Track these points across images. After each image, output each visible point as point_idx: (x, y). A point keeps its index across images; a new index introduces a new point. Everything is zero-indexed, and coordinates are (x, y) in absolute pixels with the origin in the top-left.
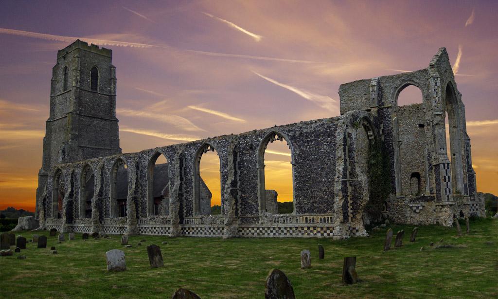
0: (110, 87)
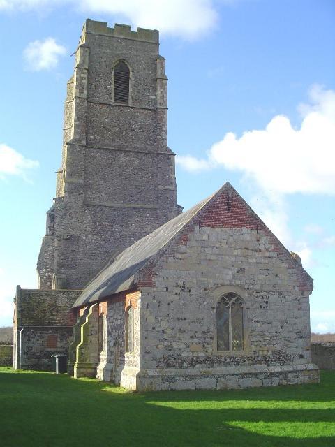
0: (156, 96)
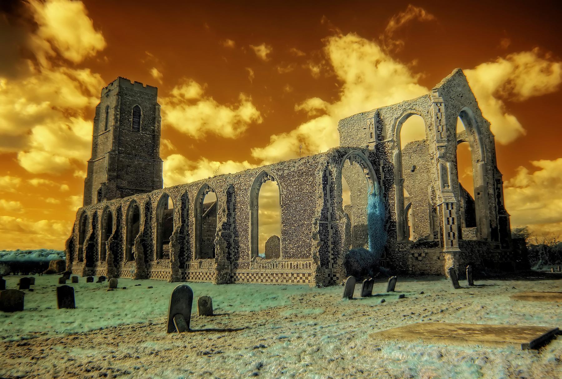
0: (154, 127)
